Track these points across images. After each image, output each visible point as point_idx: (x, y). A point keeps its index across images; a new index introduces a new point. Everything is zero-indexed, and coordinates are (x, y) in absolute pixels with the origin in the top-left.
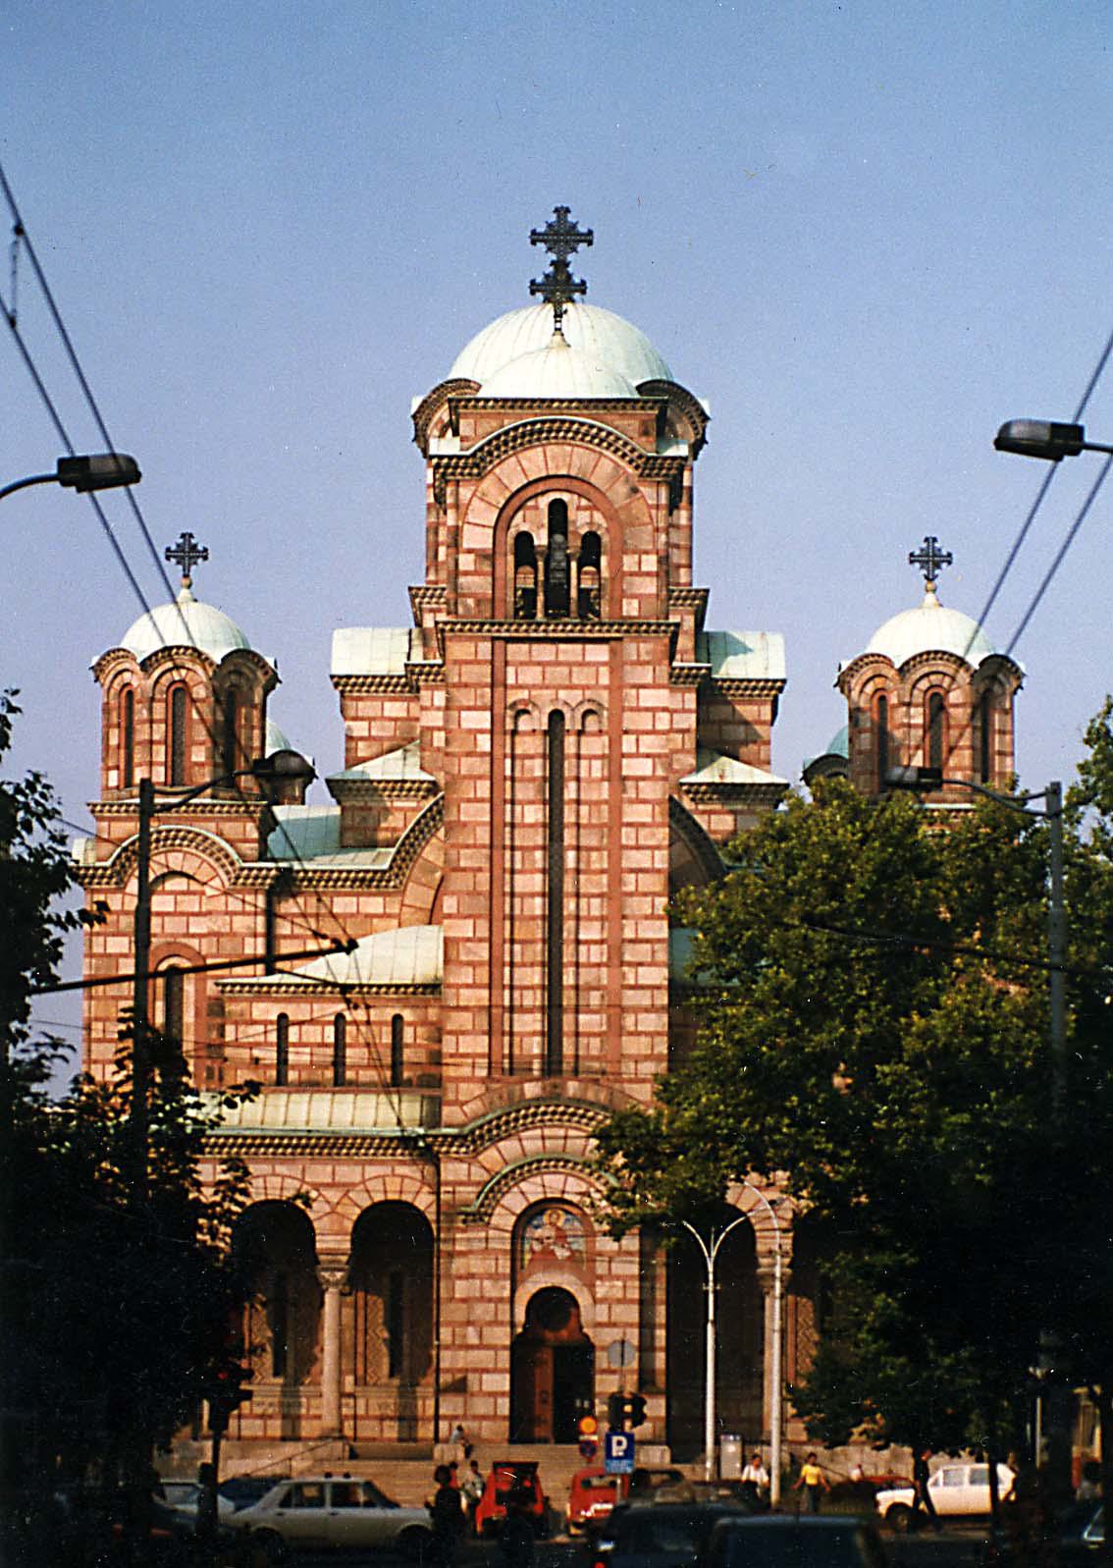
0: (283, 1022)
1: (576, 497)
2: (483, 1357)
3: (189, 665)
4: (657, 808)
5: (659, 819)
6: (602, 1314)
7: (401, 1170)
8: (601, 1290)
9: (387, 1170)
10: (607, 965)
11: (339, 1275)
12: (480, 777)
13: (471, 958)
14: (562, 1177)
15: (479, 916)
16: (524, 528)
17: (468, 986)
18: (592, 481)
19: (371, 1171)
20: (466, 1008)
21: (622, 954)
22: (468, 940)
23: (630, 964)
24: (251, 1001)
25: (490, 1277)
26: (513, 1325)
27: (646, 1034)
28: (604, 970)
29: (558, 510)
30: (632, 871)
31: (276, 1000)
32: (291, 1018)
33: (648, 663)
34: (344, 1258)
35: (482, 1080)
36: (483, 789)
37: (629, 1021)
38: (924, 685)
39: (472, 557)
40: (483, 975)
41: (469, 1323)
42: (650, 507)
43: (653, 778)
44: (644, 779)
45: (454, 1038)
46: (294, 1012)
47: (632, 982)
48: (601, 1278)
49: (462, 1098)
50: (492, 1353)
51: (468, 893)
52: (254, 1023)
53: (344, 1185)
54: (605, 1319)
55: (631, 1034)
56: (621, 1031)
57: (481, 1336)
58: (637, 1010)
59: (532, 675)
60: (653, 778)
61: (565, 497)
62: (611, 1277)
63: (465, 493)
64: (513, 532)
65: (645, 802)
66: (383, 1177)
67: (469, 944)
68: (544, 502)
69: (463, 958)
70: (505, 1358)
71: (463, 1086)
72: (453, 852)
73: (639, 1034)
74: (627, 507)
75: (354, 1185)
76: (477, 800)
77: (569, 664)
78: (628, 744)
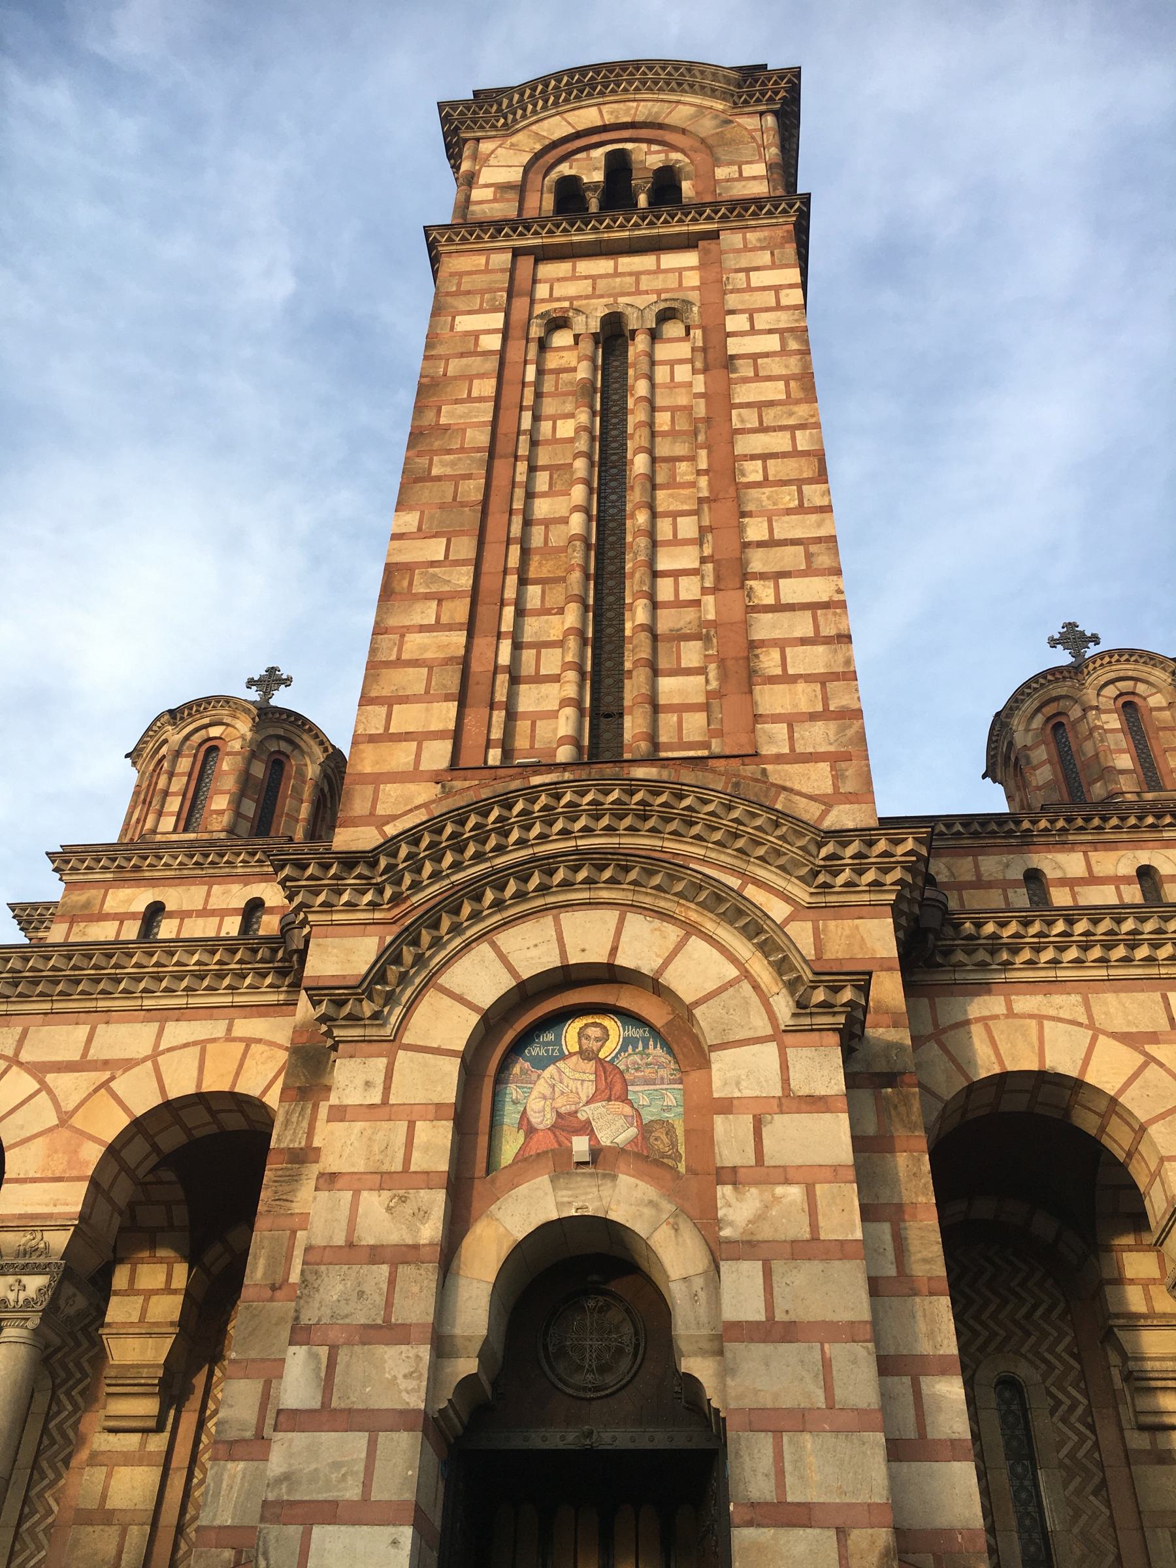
0: (156, 911)
1: (644, 146)
2: (321, 1460)
3: (227, 720)
4: (792, 384)
5: (797, 393)
6: (743, 1293)
7: (246, 1027)
8: (738, 1210)
9: (216, 1028)
10: (715, 590)
11: (34, 1283)
12: (482, 376)
13: (434, 589)
14: (612, 916)
15: (461, 533)
16: (573, 172)
17: (423, 628)
18: (667, 121)
19: (178, 1032)
20: (415, 663)
21: (742, 563)
22: (433, 564)
23: (762, 576)
24: (107, 885)
25: (383, 1180)
26: (442, 1346)
27: (808, 678)
28: (709, 601)
29: (619, 166)
30: (753, 457)
31: (153, 882)
32: (169, 907)
33: (762, 248)
34: (59, 1240)
35: (437, 778)
36: (487, 387)
37: (770, 662)
38: (1111, 691)
39: (492, 189)
40: (460, 610)
41: (300, 1334)
42: (750, 132)
43: (784, 352)
44: (767, 355)
45: (383, 710)
46: (173, 897)
47: (770, 600)
48: (731, 1176)
49: (381, 810)
50: (360, 1440)
51: (442, 506)
52: (103, 917)
53: (106, 1064)
54: (754, 1311)
55: (772, 680)
56: (750, 677)
57: (328, 1384)
58: (782, 644)
59: (571, 289)
60: (784, 352)
61: (629, 146)
62: (763, 1172)
63: (485, 147)
64: (554, 175)
65: (770, 378)
66: (203, 1044)
67: (431, 570)
68: (599, 153)
69: (419, 588)
70: (401, 1465)
71: (390, 791)
72: (424, 461)
73: (794, 679)
74: (720, 135)
75: (128, 1064)
76: (470, 399)
77: (637, 275)
78: (734, 323)
